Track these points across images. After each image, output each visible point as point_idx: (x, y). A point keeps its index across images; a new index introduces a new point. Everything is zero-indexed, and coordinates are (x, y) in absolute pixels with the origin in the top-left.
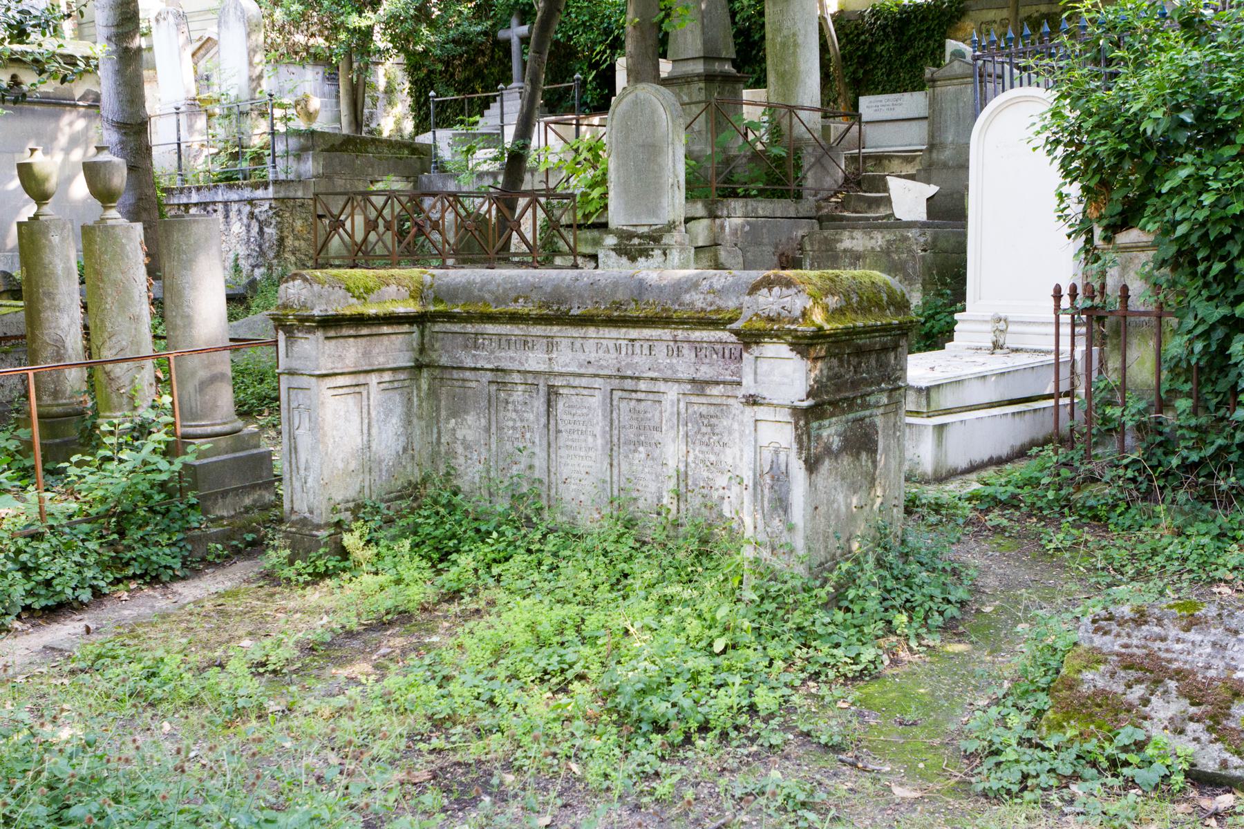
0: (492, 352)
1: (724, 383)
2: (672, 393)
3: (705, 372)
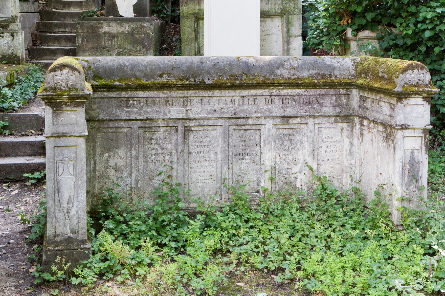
0: (141, 109)
1: (301, 117)
2: (269, 123)
3: (290, 111)
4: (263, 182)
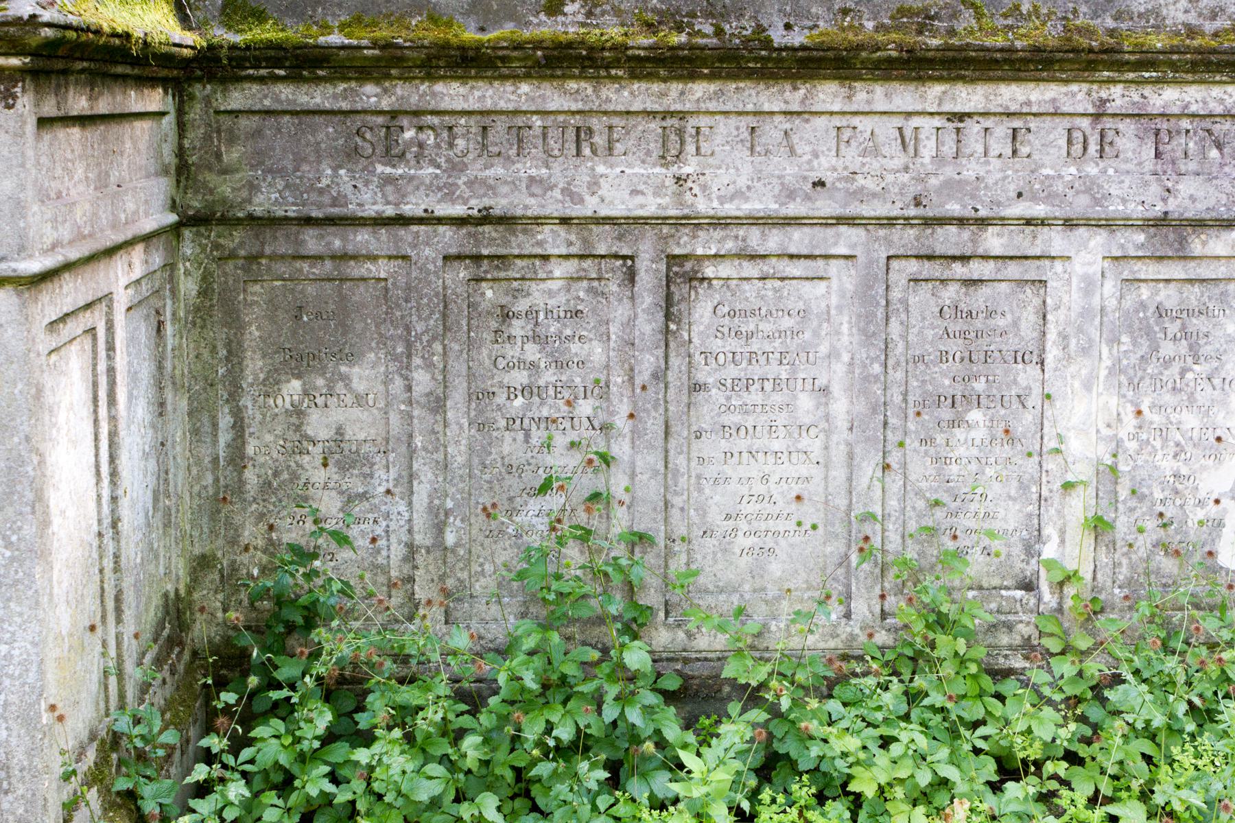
0: (456, 167)
2: (1088, 253)
3: (1193, 195)
4: (1055, 539)
